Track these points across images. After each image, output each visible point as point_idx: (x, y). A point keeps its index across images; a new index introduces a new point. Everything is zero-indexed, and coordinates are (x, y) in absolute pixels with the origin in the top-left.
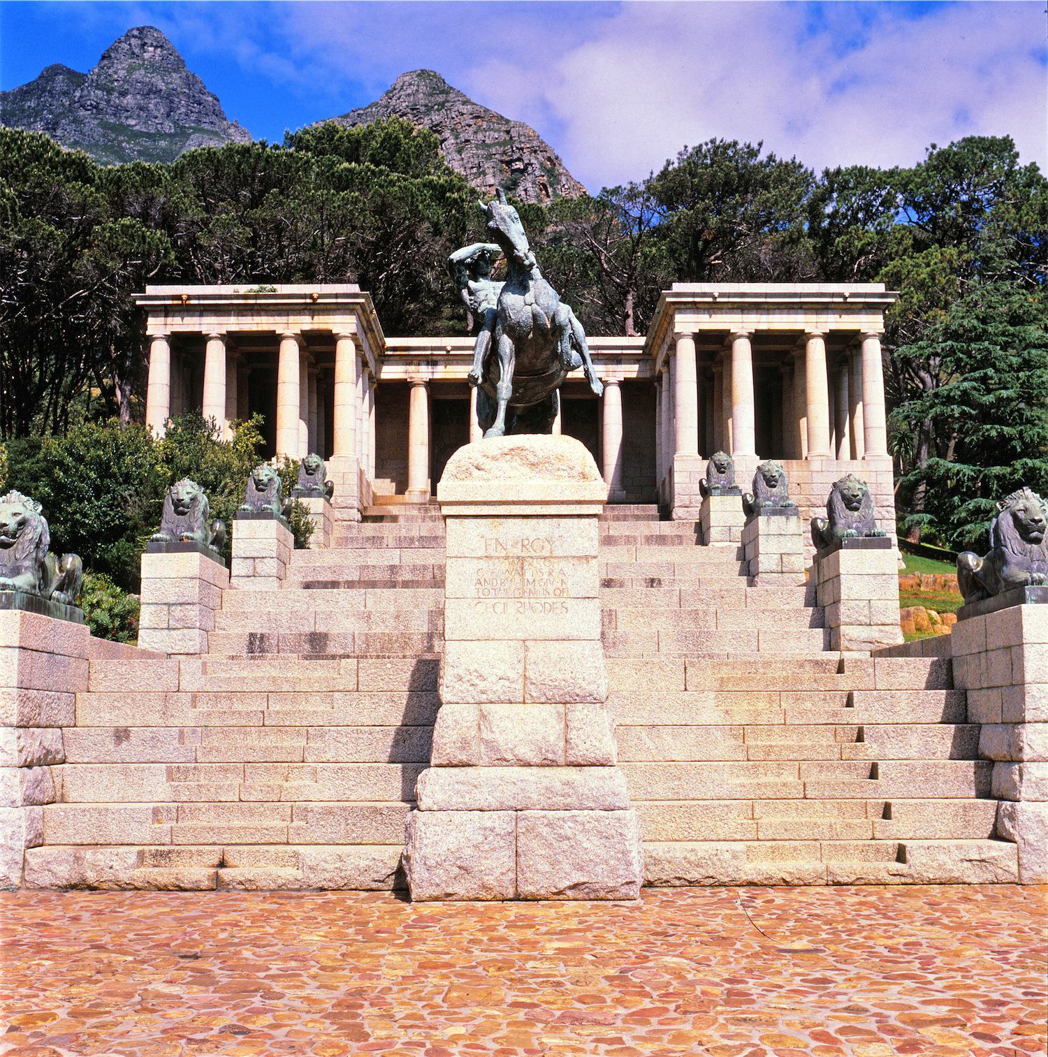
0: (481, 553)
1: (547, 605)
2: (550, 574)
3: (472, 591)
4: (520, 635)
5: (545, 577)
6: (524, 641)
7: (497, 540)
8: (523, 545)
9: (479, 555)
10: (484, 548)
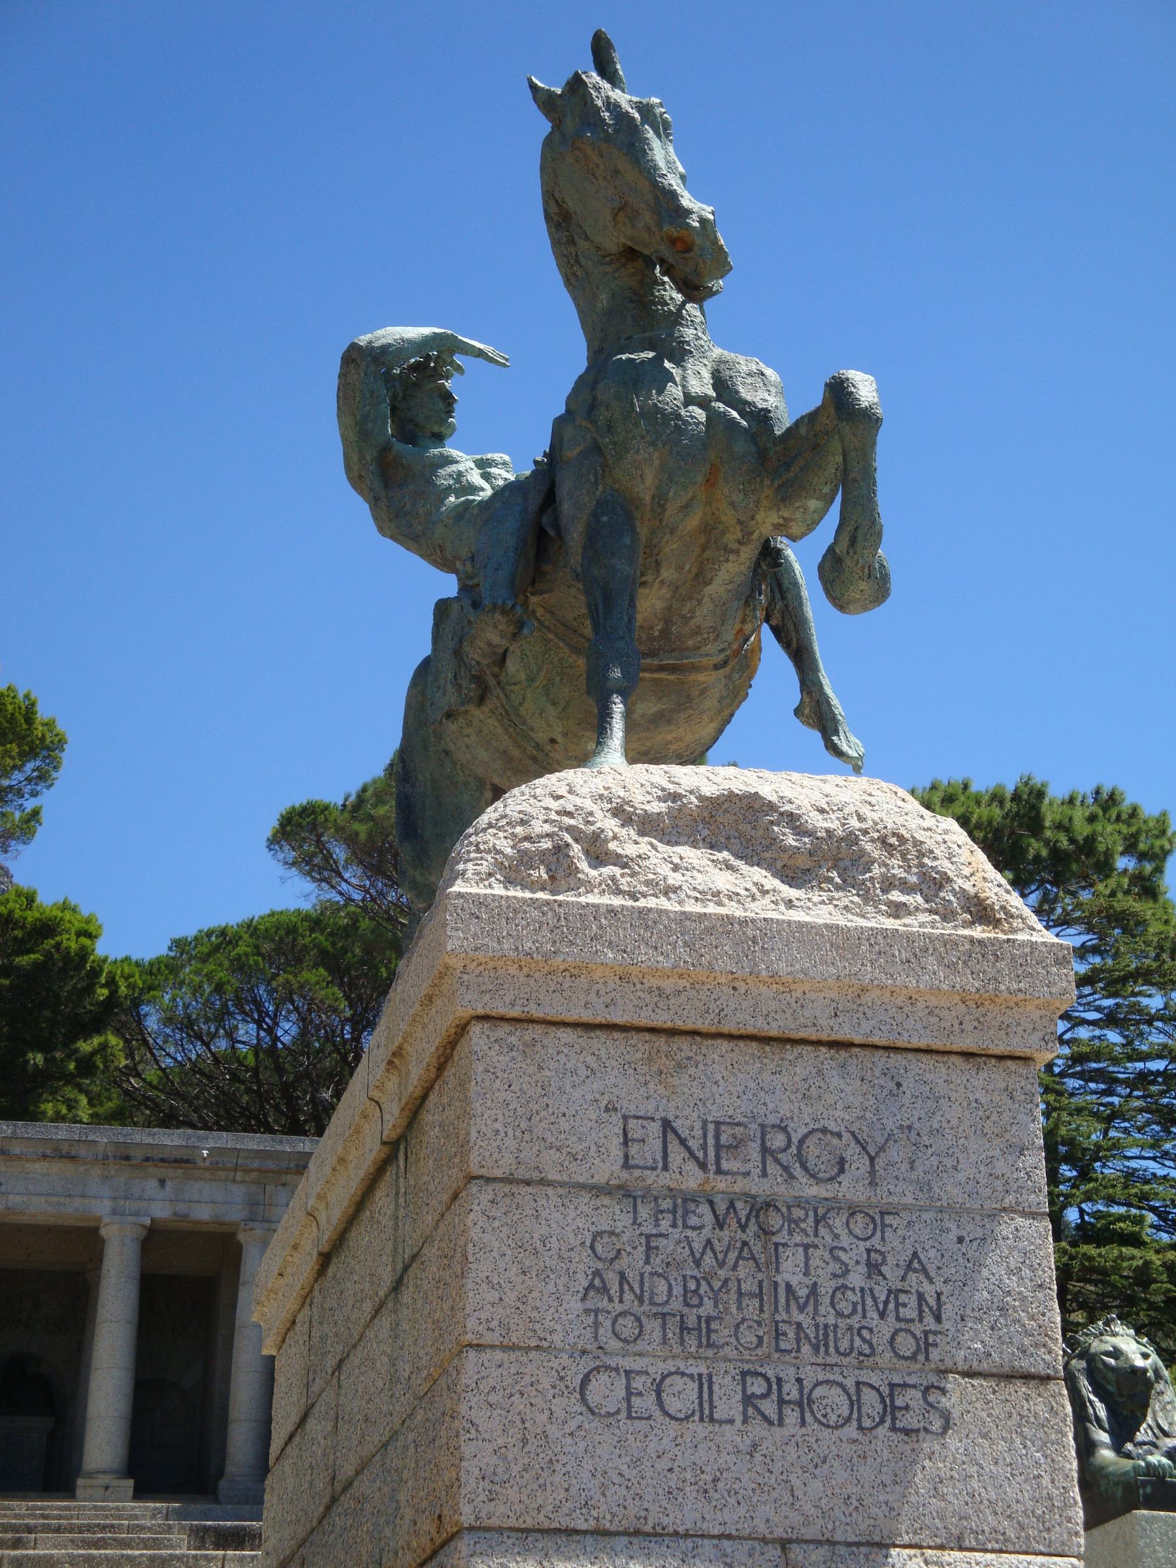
0: (607, 1169)
1: (869, 1396)
2: (874, 1268)
3: (565, 1318)
4: (770, 1517)
5: (856, 1279)
6: (784, 1544)
7: (667, 1125)
8: (765, 1150)
9: (600, 1179)
10: (616, 1152)
